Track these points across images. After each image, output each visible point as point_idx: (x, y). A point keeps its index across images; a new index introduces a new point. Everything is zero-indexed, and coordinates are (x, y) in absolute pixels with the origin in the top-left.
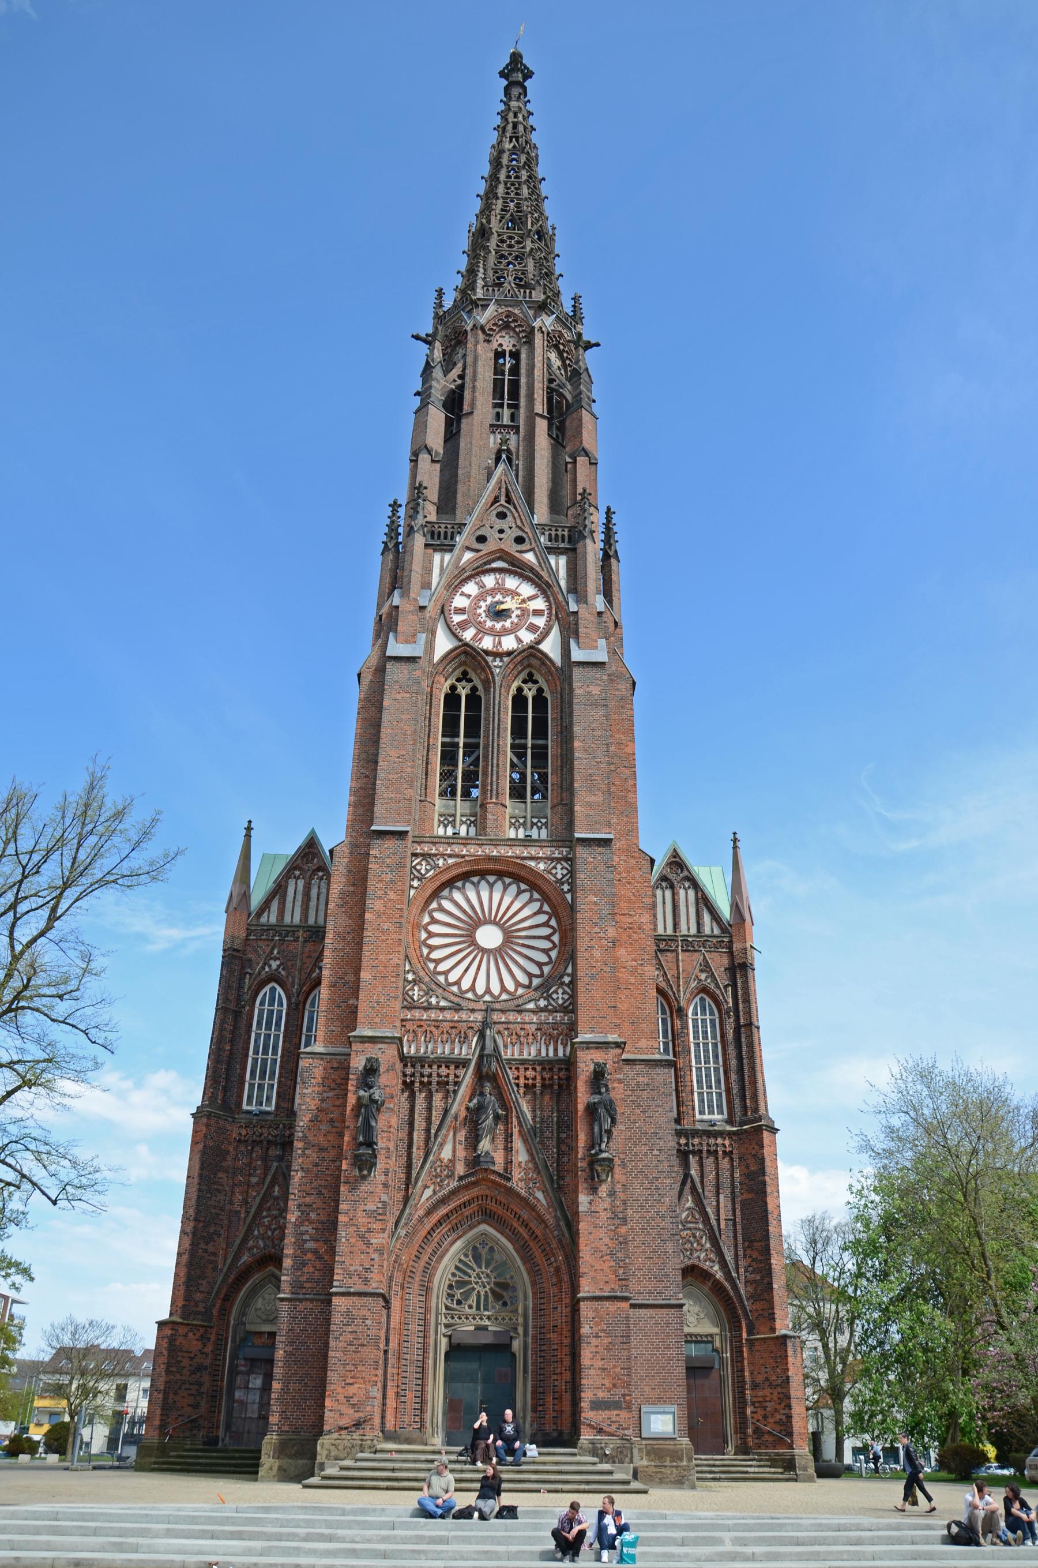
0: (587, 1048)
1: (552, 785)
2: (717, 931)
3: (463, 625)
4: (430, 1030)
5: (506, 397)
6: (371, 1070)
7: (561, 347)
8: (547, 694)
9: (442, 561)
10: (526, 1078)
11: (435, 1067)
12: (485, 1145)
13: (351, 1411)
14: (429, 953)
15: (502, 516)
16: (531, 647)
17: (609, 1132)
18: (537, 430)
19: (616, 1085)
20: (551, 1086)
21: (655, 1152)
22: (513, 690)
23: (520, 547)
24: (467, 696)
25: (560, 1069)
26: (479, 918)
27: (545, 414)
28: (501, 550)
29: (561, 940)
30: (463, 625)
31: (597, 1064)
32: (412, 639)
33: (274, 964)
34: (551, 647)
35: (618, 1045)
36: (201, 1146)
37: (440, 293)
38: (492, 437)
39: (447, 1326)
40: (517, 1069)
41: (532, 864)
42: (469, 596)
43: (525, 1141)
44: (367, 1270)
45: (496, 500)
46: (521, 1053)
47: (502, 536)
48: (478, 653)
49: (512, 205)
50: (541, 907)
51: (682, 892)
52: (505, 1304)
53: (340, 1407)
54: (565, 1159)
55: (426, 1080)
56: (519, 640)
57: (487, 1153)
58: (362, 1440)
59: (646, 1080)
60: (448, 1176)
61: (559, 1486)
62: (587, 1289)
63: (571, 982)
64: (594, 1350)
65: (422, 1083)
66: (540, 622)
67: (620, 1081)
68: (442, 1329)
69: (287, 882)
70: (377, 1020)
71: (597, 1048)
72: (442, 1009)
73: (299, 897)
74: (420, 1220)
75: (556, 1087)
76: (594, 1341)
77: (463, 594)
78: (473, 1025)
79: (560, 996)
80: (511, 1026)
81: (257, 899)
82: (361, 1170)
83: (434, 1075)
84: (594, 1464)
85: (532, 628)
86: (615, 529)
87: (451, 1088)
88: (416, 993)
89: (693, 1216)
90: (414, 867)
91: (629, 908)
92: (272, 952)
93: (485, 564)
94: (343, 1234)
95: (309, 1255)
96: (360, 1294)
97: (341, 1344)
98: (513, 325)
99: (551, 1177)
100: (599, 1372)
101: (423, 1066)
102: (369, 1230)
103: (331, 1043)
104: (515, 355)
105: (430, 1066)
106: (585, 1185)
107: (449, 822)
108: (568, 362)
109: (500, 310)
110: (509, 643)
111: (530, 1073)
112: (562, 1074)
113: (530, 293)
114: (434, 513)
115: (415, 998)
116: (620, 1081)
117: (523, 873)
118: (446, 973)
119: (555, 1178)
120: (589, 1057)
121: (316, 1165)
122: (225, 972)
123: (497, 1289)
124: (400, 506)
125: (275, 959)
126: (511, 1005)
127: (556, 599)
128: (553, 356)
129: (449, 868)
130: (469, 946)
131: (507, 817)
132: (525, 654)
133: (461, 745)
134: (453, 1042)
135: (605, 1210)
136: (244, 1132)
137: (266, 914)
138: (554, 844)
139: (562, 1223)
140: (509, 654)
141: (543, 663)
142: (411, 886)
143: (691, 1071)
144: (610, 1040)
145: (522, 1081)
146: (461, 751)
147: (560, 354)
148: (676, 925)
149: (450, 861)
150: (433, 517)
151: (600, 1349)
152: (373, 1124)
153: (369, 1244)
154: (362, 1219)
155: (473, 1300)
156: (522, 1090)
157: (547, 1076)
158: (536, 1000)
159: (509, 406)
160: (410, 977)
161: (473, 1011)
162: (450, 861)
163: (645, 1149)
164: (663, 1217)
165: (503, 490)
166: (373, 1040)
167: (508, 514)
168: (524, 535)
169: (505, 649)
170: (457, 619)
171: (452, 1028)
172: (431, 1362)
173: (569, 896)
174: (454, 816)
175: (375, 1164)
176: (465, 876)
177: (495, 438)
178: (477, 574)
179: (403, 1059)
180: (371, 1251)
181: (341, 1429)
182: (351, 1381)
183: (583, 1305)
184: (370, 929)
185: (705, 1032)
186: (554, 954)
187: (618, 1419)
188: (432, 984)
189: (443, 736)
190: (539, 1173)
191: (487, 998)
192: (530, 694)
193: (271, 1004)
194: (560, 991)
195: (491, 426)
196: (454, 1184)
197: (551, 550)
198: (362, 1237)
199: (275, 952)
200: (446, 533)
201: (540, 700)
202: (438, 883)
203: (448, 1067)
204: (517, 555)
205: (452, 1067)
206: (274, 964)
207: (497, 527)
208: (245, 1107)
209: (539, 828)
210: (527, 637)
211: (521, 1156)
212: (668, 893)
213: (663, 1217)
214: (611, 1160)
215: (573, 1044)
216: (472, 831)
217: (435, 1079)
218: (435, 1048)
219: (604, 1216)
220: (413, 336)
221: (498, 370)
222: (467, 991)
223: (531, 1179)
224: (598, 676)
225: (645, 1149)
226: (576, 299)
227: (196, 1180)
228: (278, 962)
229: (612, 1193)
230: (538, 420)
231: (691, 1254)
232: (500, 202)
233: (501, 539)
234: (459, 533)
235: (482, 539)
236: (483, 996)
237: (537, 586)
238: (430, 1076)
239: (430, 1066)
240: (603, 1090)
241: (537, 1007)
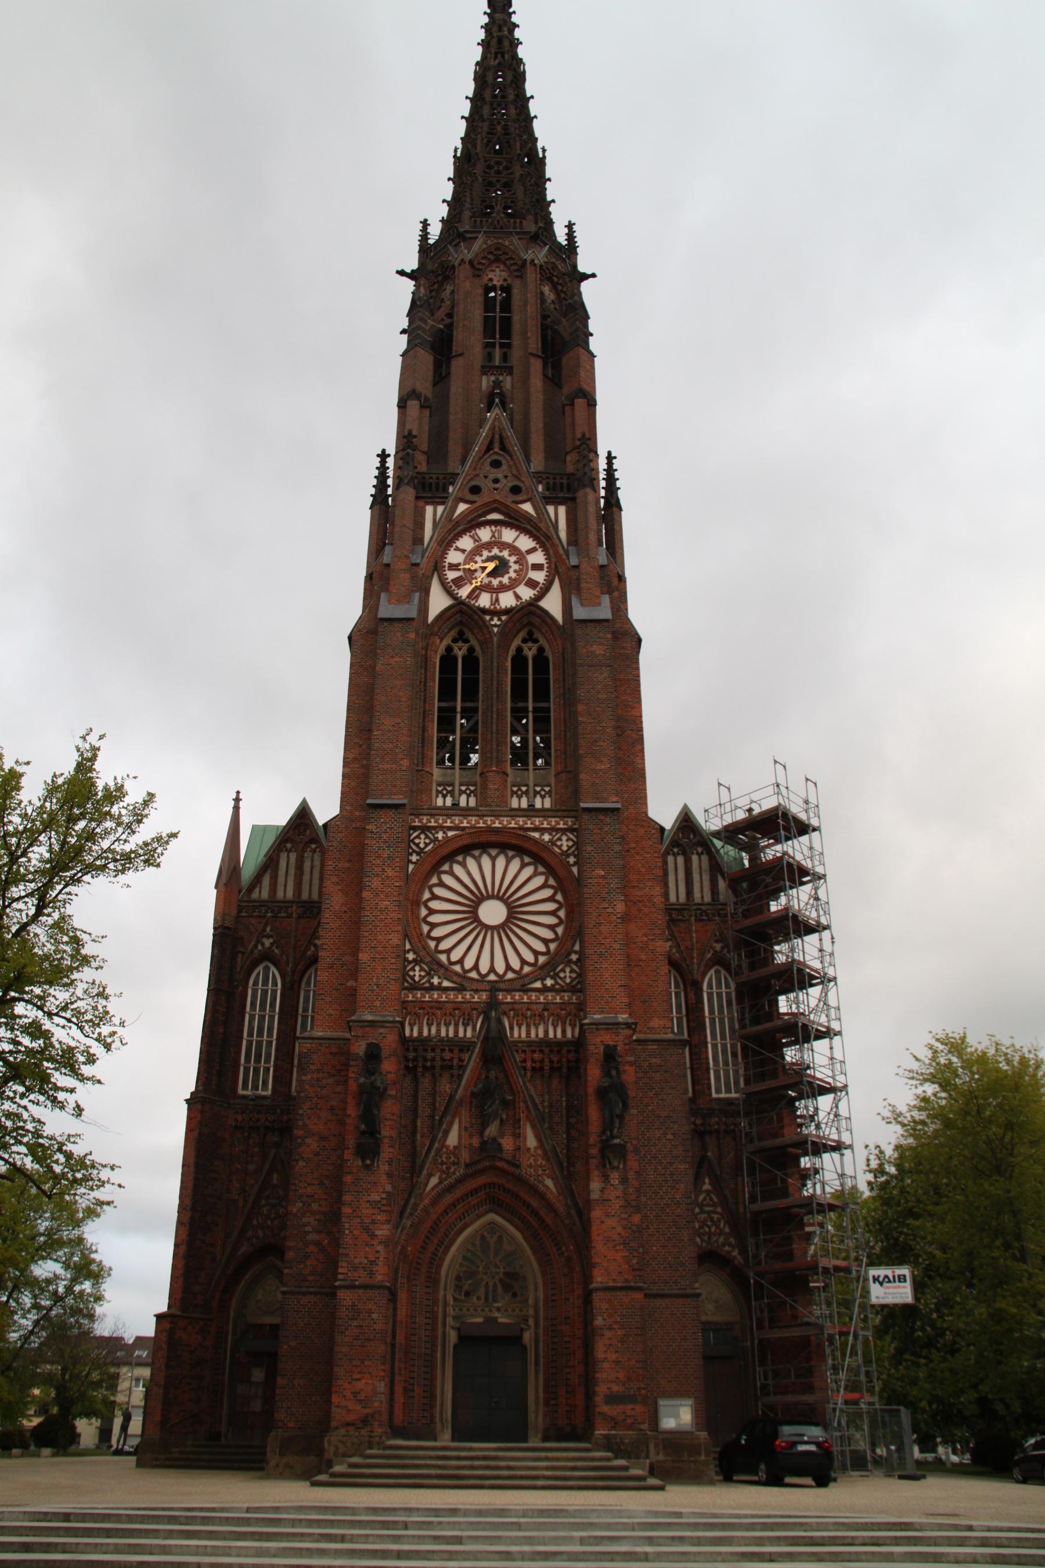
0: (597, 1029)
1: (556, 751)
4: (434, 1011)
5: (498, 336)
6: (373, 1055)
7: (555, 279)
8: (548, 653)
9: (435, 514)
10: (533, 1061)
11: (438, 1051)
12: (492, 1130)
13: (359, 1407)
14: (430, 931)
15: (496, 464)
17: (621, 1117)
18: (532, 371)
19: (627, 1068)
20: (560, 1068)
21: (669, 1136)
22: (512, 652)
24: (464, 658)
25: (569, 1051)
26: (481, 893)
27: (540, 353)
28: (496, 501)
29: (567, 915)
31: (607, 1046)
32: (406, 598)
33: (267, 942)
34: (553, 604)
35: (628, 1025)
36: (196, 1133)
37: (425, 224)
38: (484, 378)
40: (524, 1051)
41: (536, 835)
42: (463, 551)
43: (533, 1127)
44: (372, 1262)
45: (489, 447)
46: (528, 1033)
47: (497, 486)
48: (475, 612)
49: (499, 128)
50: (546, 880)
51: (695, 858)
52: (515, 1295)
54: (575, 1145)
55: (429, 1064)
57: (494, 1140)
58: (370, 1437)
59: (658, 1061)
60: (454, 1163)
62: (599, 1279)
63: (578, 960)
65: (425, 1067)
66: (540, 577)
67: (631, 1064)
69: (278, 855)
70: (378, 1003)
71: (607, 1029)
72: (447, 989)
73: (292, 871)
75: (564, 1070)
76: (608, 1334)
77: (457, 549)
78: (476, 1006)
79: (568, 974)
80: (517, 1007)
81: (247, 873)
82: (363, 1160)
83: (438, 1059)
84: (608, 1459)
85: (532, 584)
86: (617, 475)
87: (455, 1072)
88: (417, 973)
89: (711, 1199)
90: (413, 841)
92: (264, 930)
93: (481, 516)
94: (347, 1225)
95: (312, 1248)
96: (365, 1287)
97: (346, 1339)
98: (503, 257)
99: (560, 1164)
100: (613, 1366)
101: (426, 1050)
102: (373, 1222)
103: (330, 1027)
104: (507, 289)
105: (433, 1050)
106: (596, 1173)
107: (448, 792)
108: (562, 295)
109: (489, 242)
110: (507, 600)
111: (537, 1056)
112: (571, 1056)
113: (521, 223)
114: (424, 463)
115: (417, 979)
116: (631, 1064)
117: (526, 845)
118: (448, 952)
119: (565, 1164)
120: (598, 1039)
121: (317, 1154)
122: (216, 951)
124: (389, 455)
125: (268, 937)
127: (556, 553)
128: (546, 290)
129: (447, 840)
130: (471, 923)
131: (509, 785)
134: (456, 1025)
135: (618, 1197)
136: (240, 1118)
137: (257, 890)
138: (559, 814)
139: (573, 1212)
140: (507, 611)
141: (544, 622)
142: (410, 861)
143: (707, 1047)
144: (620, 1020)
145: (529, 1064)
147: (554, 287)
149: (450, 834)
150: (423, 468)
152: (376, 1112)
153: (373, 1236)
156: (529, 1074)
157: (555, 1059)
158: (543, 979)
159: (502, 345)
160: (411, 956)
161: (476, 991)
162: (450, 834)
165: (497, 436)
166: (372, 1024)
167: (504, 462)
168: (521, 484)
169: (503, 607)
172: (439, 1355)
173: (575, 870)
174: (452, 785)
175: (378, 1153)
176: (466, 850)
177: (488, 381)
179: (404, 1041)
180: (375, 1242)
181: (348, 1424)
182: (358, 1376)
183: (596, 1297)
184: (367, 908)
185: (720, 1006)
186: (560, 930)
187: (633, 1413)
188: (435, 966)
189: (439, 701)
190: (548, 1160)
191: (492, 977)
192: (530, 653)
193: (265, 982)
194: (568, 970)
195: (482, 367)
196: (461, 1171)
197: (548, 500)
198: (367, 1229)
199: (268, 929)
200: (437, 484)
201: (541, 660)
203: (451, 1051)
204: (513, 506)
205: (456, 1051)
206: (267, 942)
207: (491, 476)
208: (240, 1091)
209: (543, 797)
210: (526, 593)
211: (531, 1142)
212: (680, 859)
214: (622, 1147)
215: (582, 1026)
216: (472, 802)
217: (438, 1063)
218: (439, 1031)
219: (616, 1205)
220: (398, 272)
221: (489, 305)
223: (541, 1166)
224: (601, 635)
226: (570, 226)
227: (192, 1169)
228: (271, 940)
229: (624, 1180)
230: (533, 360)
231: (709, 1238)
232: (486, 124)
233: (496, 489)
234: (452, 484)
235: (476, 490)
237: (535, 538)
238: (433, 1059)
239: (433, 1050)
240: (614, 1073)
241: (544, 985)
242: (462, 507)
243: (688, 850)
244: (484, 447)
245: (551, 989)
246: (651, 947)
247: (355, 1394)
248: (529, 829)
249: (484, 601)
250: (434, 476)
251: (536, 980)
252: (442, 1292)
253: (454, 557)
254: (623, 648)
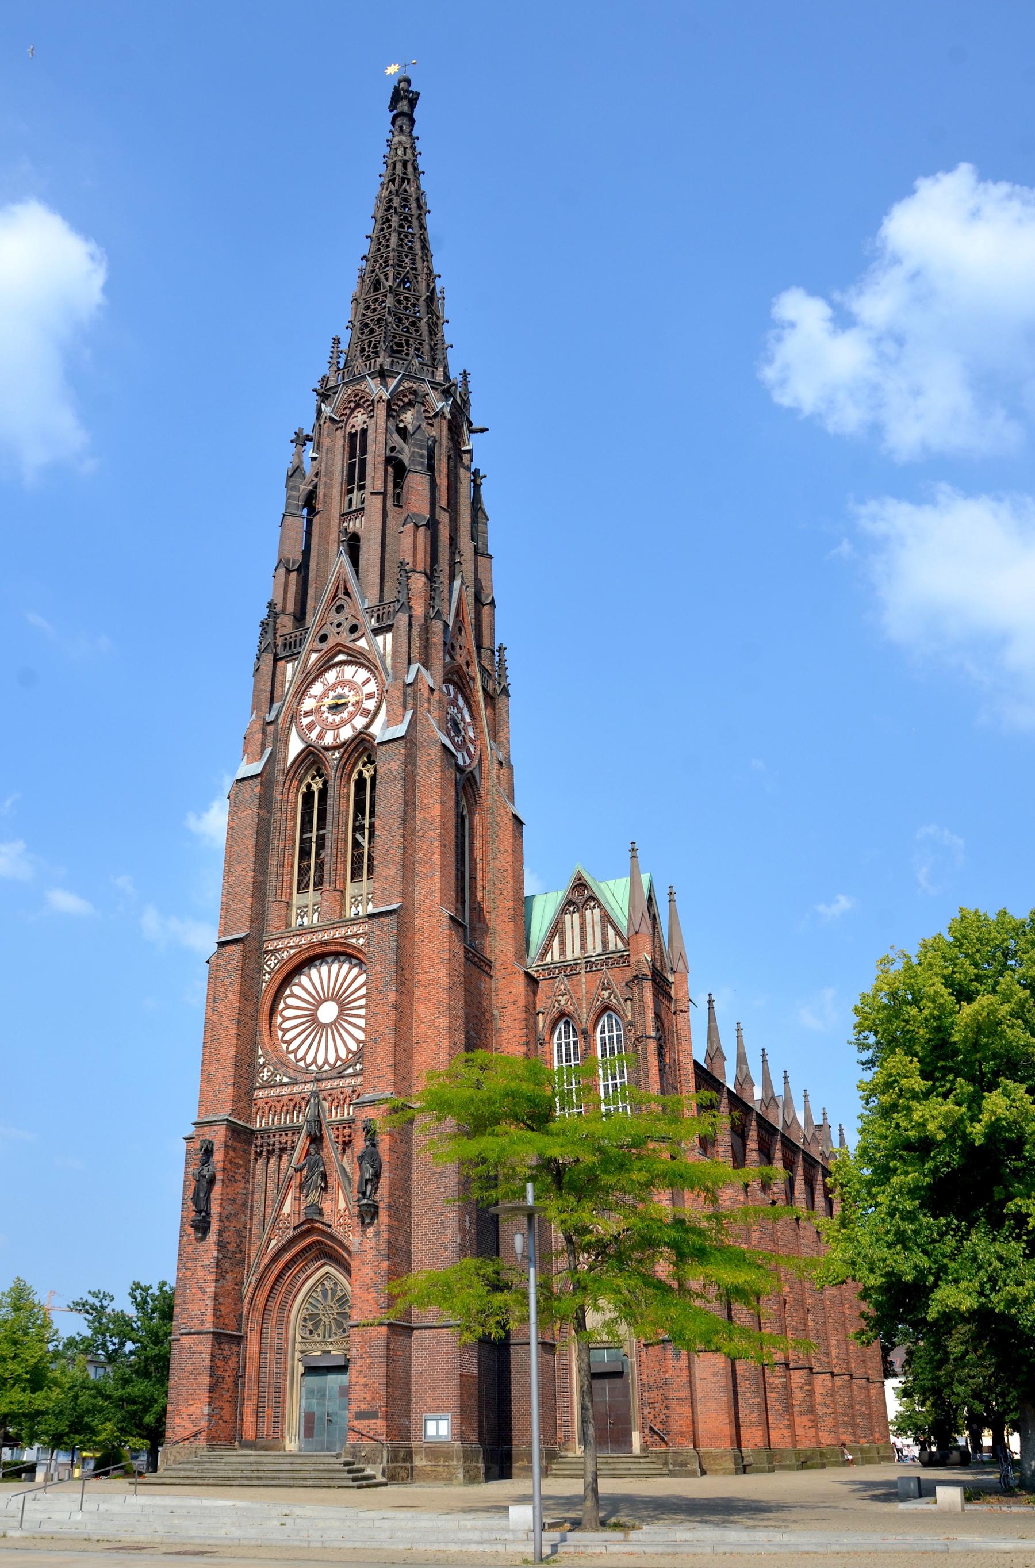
2: (620, 946)
3: (311, 727)
11: (277, 1136)
16: (361, 733)
22: (355, 776)
23: (353, 636)
28: (338, 645)
30: (311, 727)
39: (302, 1352)
40: (337, 1129)
52: (344, 1331)
53: (184, 1423)
55: (271, 1148)
56: (354, 728)
61: (292, 1482)
64: (359, 1369)
68: (298, 1355)
74: (268, 1267)
76: (359, 1362)
80: (334, 1092)
83: (277, 1143)
85: (365, 713)
91: (430, 966)
93: (328, 661)
97: (186, 1374)
109: (349, 392)
110: (346, 733)
123: (339, 1319)
126: (334, 1073)
132: (357, 741)
133: (314, 839)
145: (341, 1139)
146: (314, 845)
148: (583, 947)
149: (292, 952)
151: (364, 1368)
154: (200, 1273)
155: (321, 1331)
162: (292, 952)
163: (433, 1187)
164: (446, 1247)
170: (305, 721)
171: (291, 1100)
172: (288, 1383)
178: (321, 674)
187: (375, 1426)
196: (291, 1233)
198: (200, 1287)
202: (284, 974)
203: (287, 1135)
205: (290, 1133)
207: (336, 622)
210: (360, 722)
212: (576, 916)
213: (446, 1247)
222: (311, 1065)
225: (433, 1187)
229: (377, 1234)
236: (322, 1067)
237: (370, 670)
242: (314, 656)
243: (580, 905)
244: (331, 596)
246: (436, 1024)
249: (329, 739)
250: (293, 635)
251: (348, 1067)
252: (291, 1332)
253: (308, 704)
254: (429, 755)
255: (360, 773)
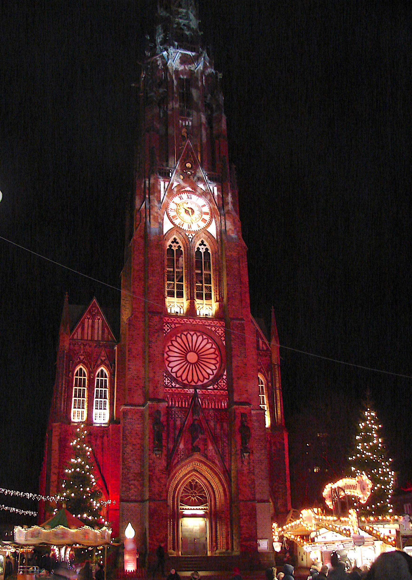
41: (209, 328)
76: (245, 517)
121: (132, 451)
149: (177, 325)
192: (202, 251)
245: (216, 389)
247: (156, 539)
248: (207, 325)
255: (198, 249)
